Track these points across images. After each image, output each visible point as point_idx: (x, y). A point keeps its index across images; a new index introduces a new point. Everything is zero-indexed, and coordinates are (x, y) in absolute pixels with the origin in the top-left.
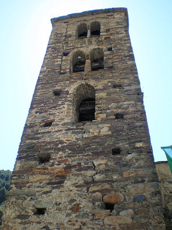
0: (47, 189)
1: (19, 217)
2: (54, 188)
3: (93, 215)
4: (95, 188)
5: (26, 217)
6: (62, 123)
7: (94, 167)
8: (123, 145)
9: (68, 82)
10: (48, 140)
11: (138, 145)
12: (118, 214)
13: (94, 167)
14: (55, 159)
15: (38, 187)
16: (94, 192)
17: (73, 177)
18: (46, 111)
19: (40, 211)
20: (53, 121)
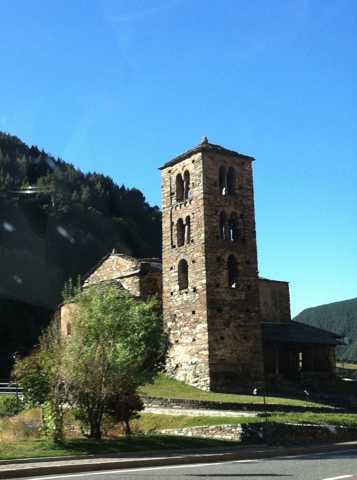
0: (224, 327)
1: (215, 340)
2: (226, 327)
3: (241, 341)
4: (241, 329)
5: (218, 340)
6: (224, 286)
7: (239, 318)
8: (250, 307)
9: (223, 250)
10: (219, 297)
11: (256, 308)
12: (248, 342)
13: (239, 318)
14: (224, 311)
15: (220, 326)
16: (241, 331)
17: (232, 322)
18: (215, 275)
19: (222, 338)
20: (219, 284)
